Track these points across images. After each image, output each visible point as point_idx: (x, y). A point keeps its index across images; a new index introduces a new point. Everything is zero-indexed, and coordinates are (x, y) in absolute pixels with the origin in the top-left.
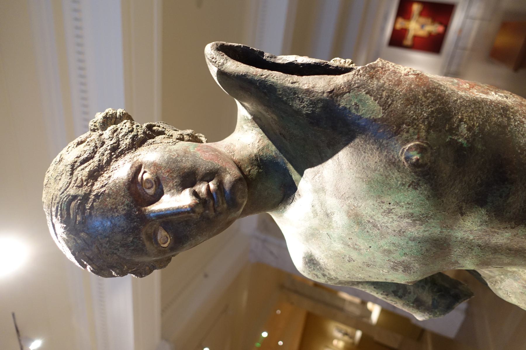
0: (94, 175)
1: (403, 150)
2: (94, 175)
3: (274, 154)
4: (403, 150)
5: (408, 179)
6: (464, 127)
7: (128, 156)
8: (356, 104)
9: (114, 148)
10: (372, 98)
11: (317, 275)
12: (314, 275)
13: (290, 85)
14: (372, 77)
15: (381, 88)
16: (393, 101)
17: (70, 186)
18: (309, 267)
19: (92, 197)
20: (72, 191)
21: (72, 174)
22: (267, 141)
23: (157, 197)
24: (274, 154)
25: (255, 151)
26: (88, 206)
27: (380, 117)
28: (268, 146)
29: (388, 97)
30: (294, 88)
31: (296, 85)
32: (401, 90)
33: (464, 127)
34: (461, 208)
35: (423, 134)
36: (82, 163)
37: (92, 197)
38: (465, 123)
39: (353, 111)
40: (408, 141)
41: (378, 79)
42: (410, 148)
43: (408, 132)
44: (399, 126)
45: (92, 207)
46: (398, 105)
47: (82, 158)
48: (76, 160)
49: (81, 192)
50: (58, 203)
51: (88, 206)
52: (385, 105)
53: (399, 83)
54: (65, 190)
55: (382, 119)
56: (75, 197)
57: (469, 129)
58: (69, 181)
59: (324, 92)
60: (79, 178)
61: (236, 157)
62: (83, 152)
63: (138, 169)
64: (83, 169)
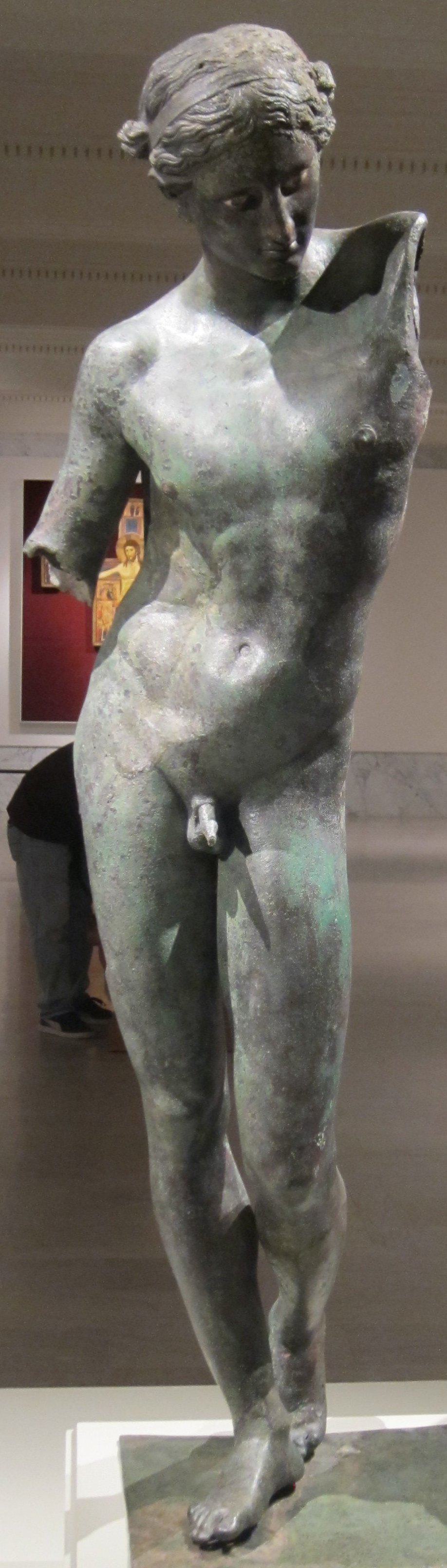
0: (305, 127)
1: (369, 427)
3: (302, 294)
4: (369, 427)
5: (341, 439)
6: (389, 474)
8: (400, 378)
10: (405, 391)
11: (117, 374)
12: (115, 370)
13: (406, 314)
14: (421, 387)
16: (405, 409)
17: (295, 105)
18: (130, 363)
19: (288, 132)
20: (293, 112)
22: (313, 282)
23: (286, 193)
24: (302, 294)
26: (282, 131)
27: (393, 400)
28: (309, 285)
29: (408, 404)
30: (405, 319)
31: (407, 320)
34: (316, 493)
35: (383, 440)
36: (313, 108)
37: (288, 132)
38: (393, 475)
39: (394, 377)
40: (376, 429)
41: (420, 393)
42: (370, 432)
43: (384, 427)
44: (387, 419)
45: (280, 135)
46: (403, 414)
47: (315, 105)
48: (314, 100)
50: (278, 95)
51: (282, 131)
52: (402, 404)
54: (291, 100)
55: (391, 403)
56: (287, 115)
57: (389, 479)
58: (299, 102)
59: (406, 347)
62: (318, 103)
64: (309, 112)
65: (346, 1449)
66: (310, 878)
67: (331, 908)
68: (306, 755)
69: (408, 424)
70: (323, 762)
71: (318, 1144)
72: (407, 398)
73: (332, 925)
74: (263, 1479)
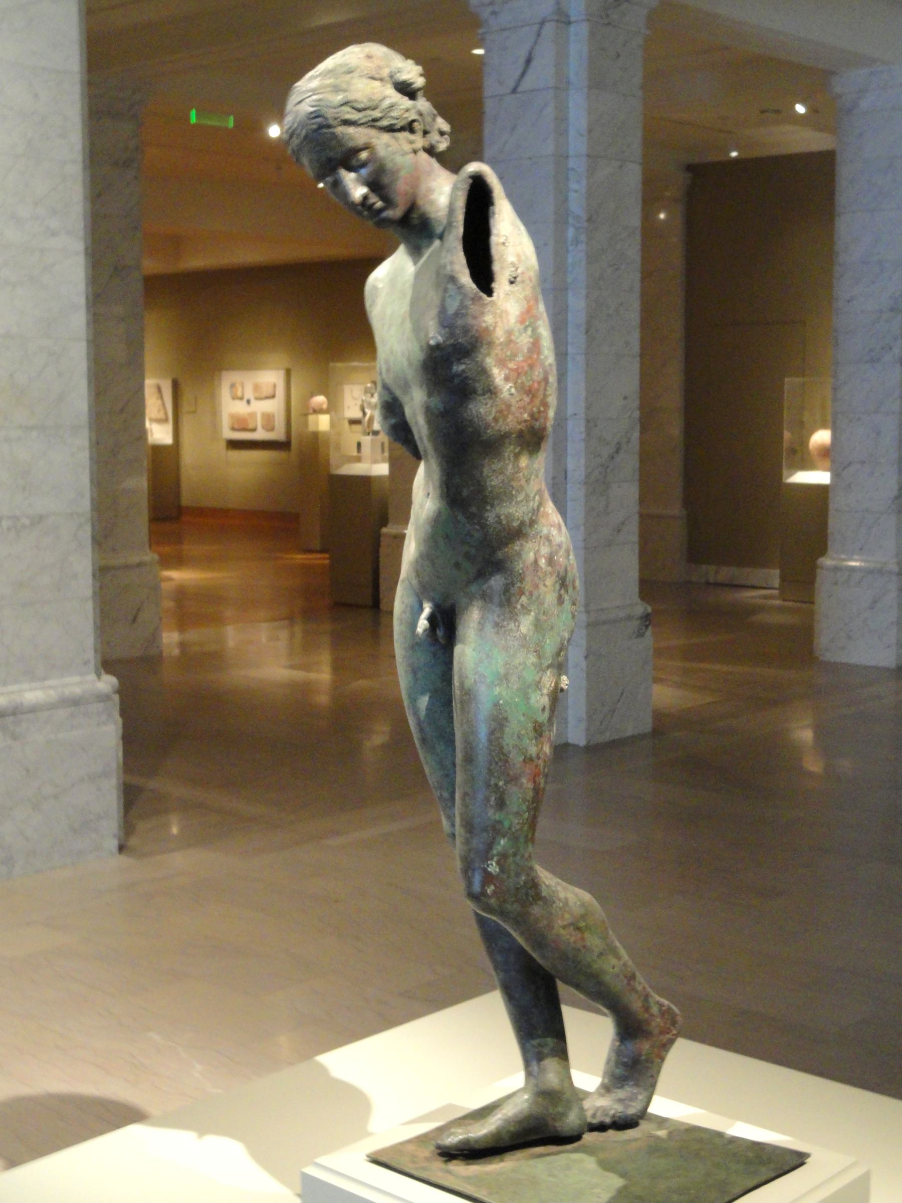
0: (347, 123)
2: (347, 123)
6: (463, 367)
7: (373, 132)
9: (375, 120)
15: (466, 307)
20: (329, 116)
21: (342, 105)
25: (433, 216)
29: (462, 314)
32: (470, 321)
33: (463, 367)
35: (448, 343)
36: (354, 108)
41: (473, 304)
46: (460, 322)
49: (331, 122)
52: (456, 314)
53: (475, 318)
56: (326, 119)
57: (463, 371)
60: (339, 115)
61: (420, 202)
63: (366, 147)
64: (348, 113)
65: (662, 1133)
66: (479, 669)
67: (496, 693)
68: (482, 575)
69: (466, 330)
70: (496, 582)
71: (489, 869)
72: (461, 310)
73: (496, 705)
74: (507, 1121)
